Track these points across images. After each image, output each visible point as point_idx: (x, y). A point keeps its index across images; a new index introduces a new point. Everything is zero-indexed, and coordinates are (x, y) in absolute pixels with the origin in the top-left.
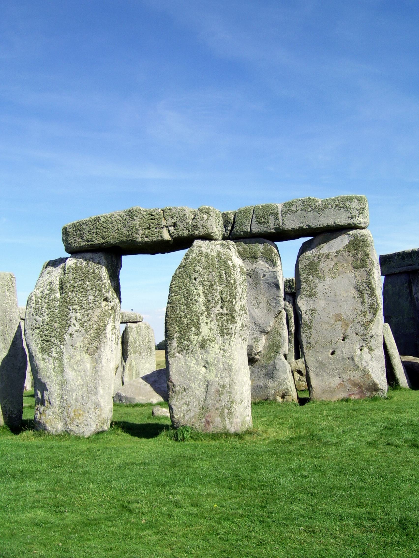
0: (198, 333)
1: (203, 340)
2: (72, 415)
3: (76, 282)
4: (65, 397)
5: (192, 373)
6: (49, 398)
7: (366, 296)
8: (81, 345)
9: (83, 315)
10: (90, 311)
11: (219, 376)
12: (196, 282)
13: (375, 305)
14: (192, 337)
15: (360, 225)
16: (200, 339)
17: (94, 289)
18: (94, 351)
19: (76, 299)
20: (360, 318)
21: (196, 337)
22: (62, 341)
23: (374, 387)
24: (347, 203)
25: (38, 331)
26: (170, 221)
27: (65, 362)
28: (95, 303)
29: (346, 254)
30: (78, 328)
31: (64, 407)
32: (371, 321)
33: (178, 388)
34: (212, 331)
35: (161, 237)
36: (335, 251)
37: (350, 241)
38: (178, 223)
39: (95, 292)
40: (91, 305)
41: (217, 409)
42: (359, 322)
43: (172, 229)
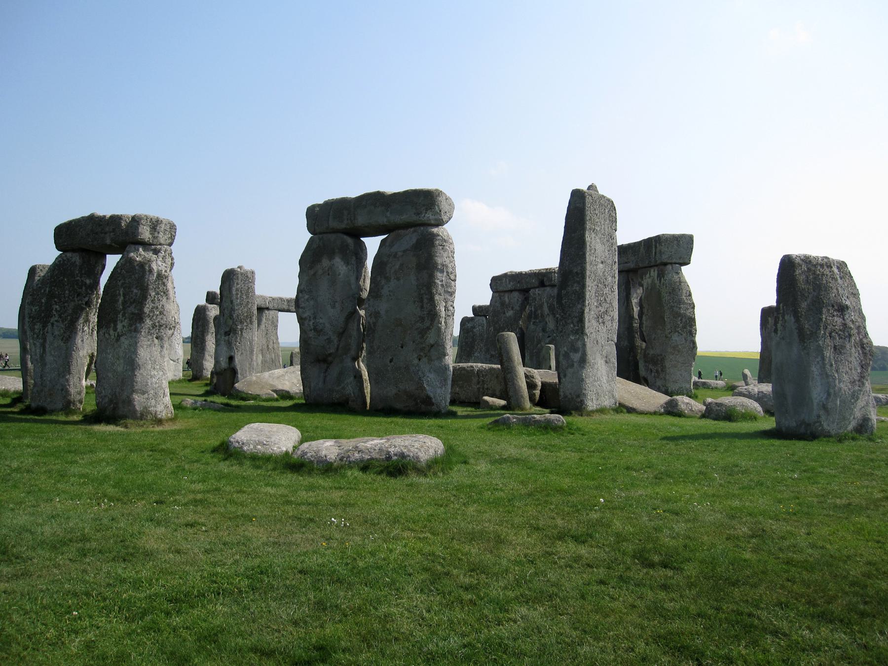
0: (115, 330)
1: (118, 335)
7: (425, 301)
20: (419, 325)
23: (428, 401)
27: (47, 346)
32: (428, 328)
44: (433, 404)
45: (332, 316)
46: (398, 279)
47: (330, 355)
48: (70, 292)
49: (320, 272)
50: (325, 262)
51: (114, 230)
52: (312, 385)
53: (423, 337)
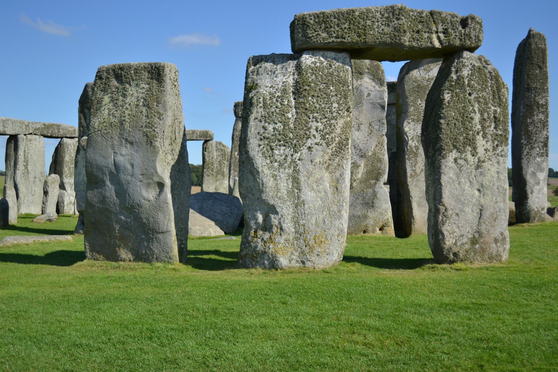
2: (312, 242)
4: (302, 222)
6: (280, 223)
8: (321, 160)
10: (333, 121)
11: (494, 200)
16: (476, 160)
17: (339, 96)
18: (335, 169)
19: (318, 106)
28: (340, 112)
30: (319, 141)
31: (300, 234)
33: (450, 212)
34: (488, 153)
35: (431, 43)
38: (450, 30)
40: (334, 114)
43: (441, 35)
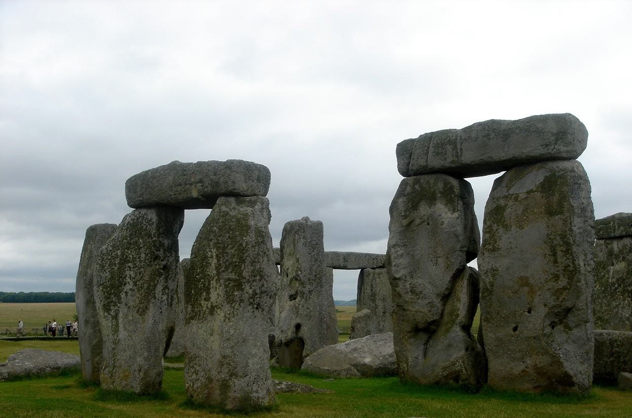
0: (207, 299)
1: (212, 306)
3: (131, 239)
5: (201, 341)
7: (559, 254)
9: (136, 273)
10: (142, 270)
12: (211, 243)
13: (570, 266)
14: (203, 302)
15: (560, 155)
20: (552, 284)
21: (207, 303)
22: (119, 298)
23: (566, 381)
24: (540, 125)
25: (101, 289)
26: (198, 177)
27: (120, 320)
29: (538, 195)
36: (526, 191)
37: (546, 177)
39: (146, 250)
40: (143, 264)
41: (218, 381)
42: (549, 289)
44: (572, 384)
45: (434, 276)
46: (521, 227)
47: (433, 322)
48: (146, 255)
49: (418, 221)
50: (424, 210)
51: (201, 181)
52: (410, 359)
53: (557, 299)
